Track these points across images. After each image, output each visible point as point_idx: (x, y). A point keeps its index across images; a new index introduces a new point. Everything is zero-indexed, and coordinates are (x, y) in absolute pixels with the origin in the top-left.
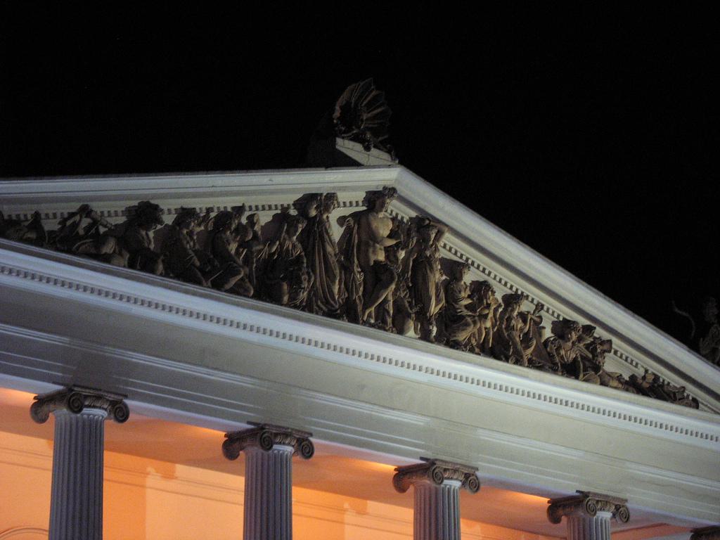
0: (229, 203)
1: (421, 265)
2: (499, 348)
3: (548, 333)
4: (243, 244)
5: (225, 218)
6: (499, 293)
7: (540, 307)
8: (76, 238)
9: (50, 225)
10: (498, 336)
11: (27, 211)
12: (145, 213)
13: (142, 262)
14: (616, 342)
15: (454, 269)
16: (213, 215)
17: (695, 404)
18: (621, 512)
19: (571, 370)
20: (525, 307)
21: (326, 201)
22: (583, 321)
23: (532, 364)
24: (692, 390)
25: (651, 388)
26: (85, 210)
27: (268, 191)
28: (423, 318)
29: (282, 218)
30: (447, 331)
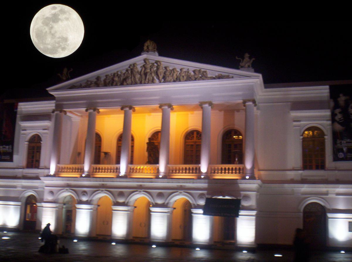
0: (115, 71)
1: (158, 68)
2: (178, 80)
3: (192, 73)
4: (119, 77)
5: (114, 74)
6: (179, 70)
7: (188, 69)
8: (88, 85)
9: (83, 85)
10: (177, 79)
11: (79, 84)
12: (98, 78)
13: (106, 84)
14: (207, 70)
15: (166, 68)
16: (113, 74)
17: (233, 77)
18: (210, 104)
19: (196, 79)
20: (184, 70)
21: (134, 65)
22: (198, 69)
23: (186, 81)
24: (231, 75)
25: (220, 77)
26: (88, 81)
27: (122, 66)
28: (159, 79)
29: (127, 70)
30: (165, 80)
